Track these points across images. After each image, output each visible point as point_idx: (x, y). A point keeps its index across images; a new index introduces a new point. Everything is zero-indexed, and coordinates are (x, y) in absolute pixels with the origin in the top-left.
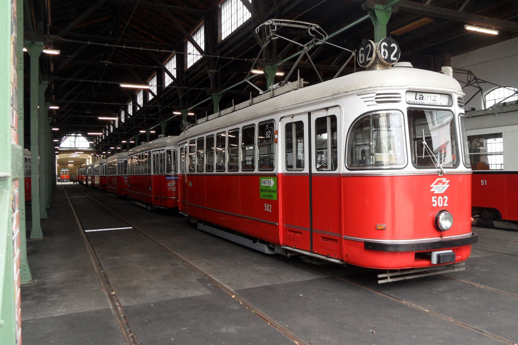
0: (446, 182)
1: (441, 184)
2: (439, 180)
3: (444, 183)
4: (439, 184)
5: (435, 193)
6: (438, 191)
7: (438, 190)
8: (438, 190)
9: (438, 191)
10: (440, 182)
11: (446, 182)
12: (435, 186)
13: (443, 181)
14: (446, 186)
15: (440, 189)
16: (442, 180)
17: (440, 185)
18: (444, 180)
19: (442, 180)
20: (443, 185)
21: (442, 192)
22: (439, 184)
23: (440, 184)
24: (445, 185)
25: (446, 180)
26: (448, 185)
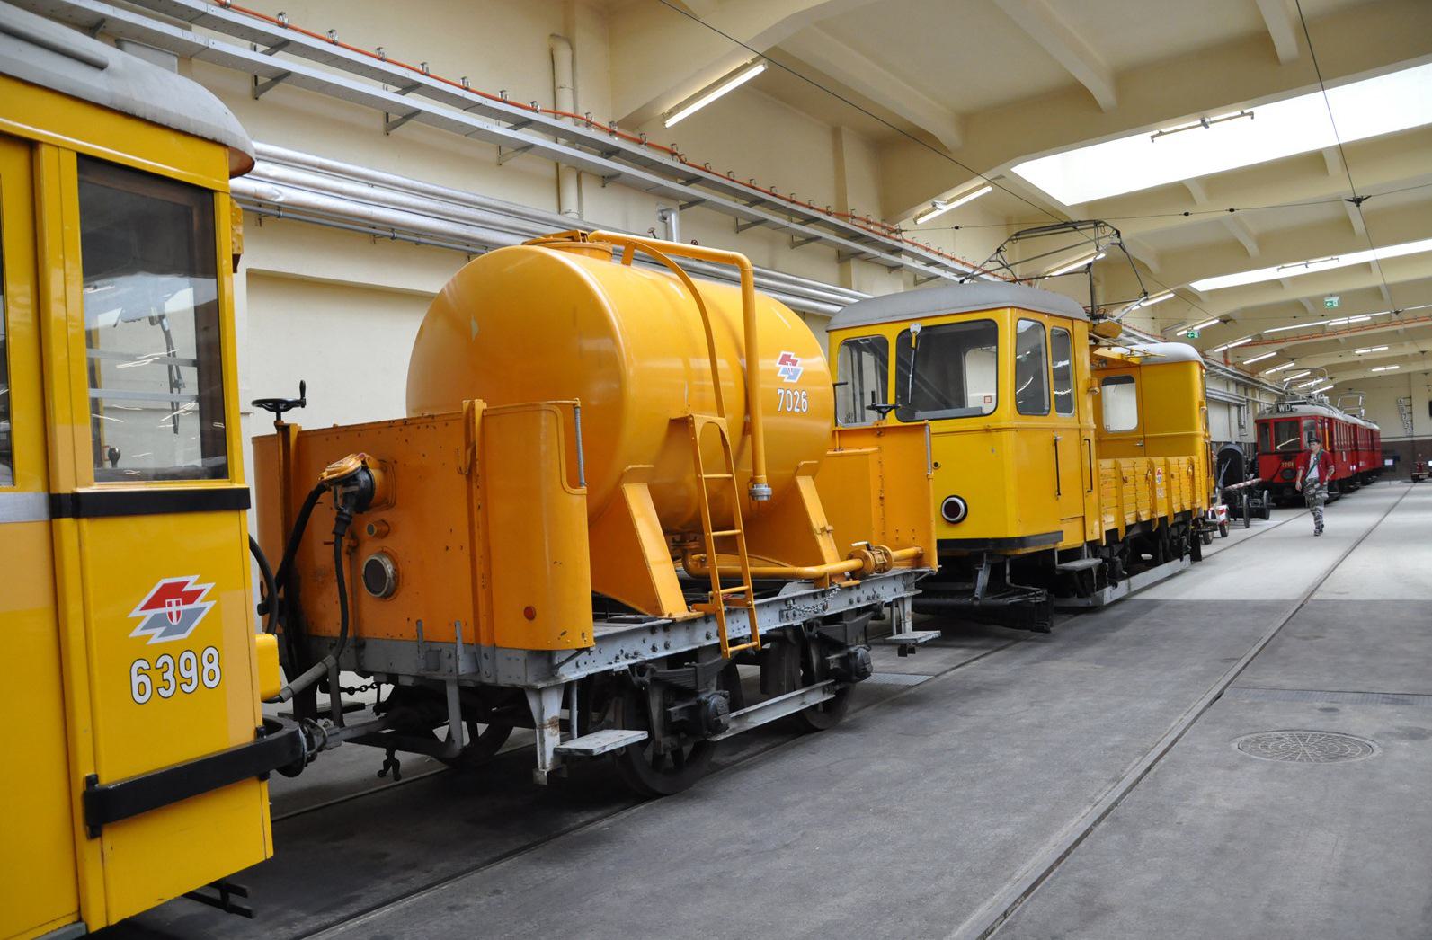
1: (178, 604)
4: (167, 601)
5: (151, 642)
6: (162, 635)
7: (163, 628)
8: (162, 630)
9: (162, 635)
12: (151, 613)
13: (187, 588)
15: (175, 622)
16: (185, 583)
19: (185, 583)
20: (184, 604)
22: (170, 605)
23: (173, 601)
24: (197, 604)
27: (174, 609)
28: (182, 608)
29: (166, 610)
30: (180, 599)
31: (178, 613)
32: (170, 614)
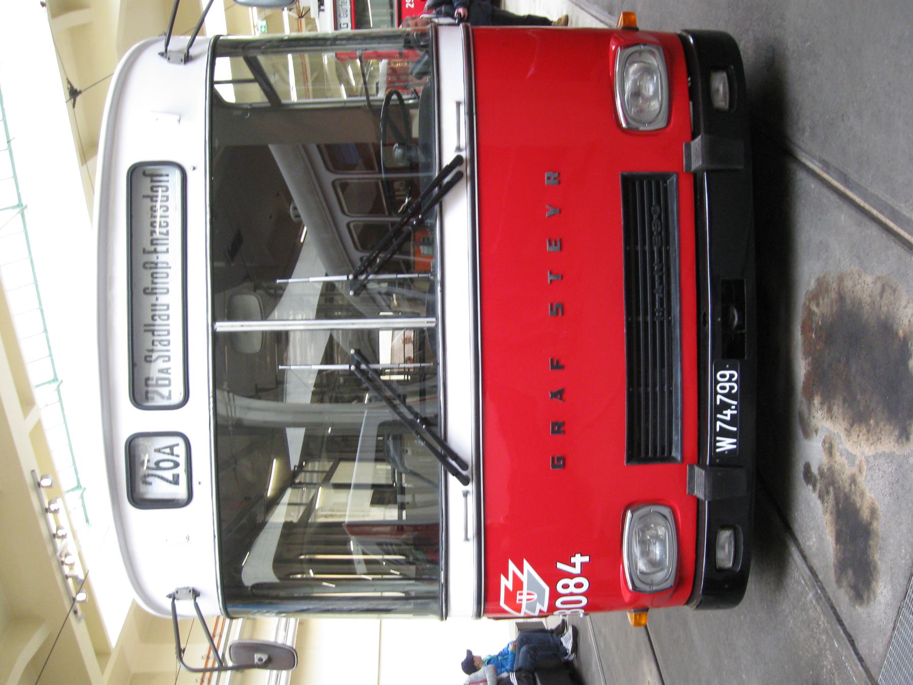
0: (515, 575)
1: (521, 594)
2: (506, 602)
3: (518, 584)
4: (517, 602)
10: (511, 597)
11: (515, 575)
13: (511, 588)
14: (529, 574)
16: (506, 588)
17: (523, 598)
18: (506, 583)
19: (506, 588)
20: (522, 589)
21: (547, 589)
22: (521, 600)
23: (518, 597)
24: (524, 578)
25: (507, 577)
26: (526, 565)
27: (525, 597)
28: (525, 591)
29: (524, 603)
30: (518, 592)
31: (528, 594)
32: (528, 600)
